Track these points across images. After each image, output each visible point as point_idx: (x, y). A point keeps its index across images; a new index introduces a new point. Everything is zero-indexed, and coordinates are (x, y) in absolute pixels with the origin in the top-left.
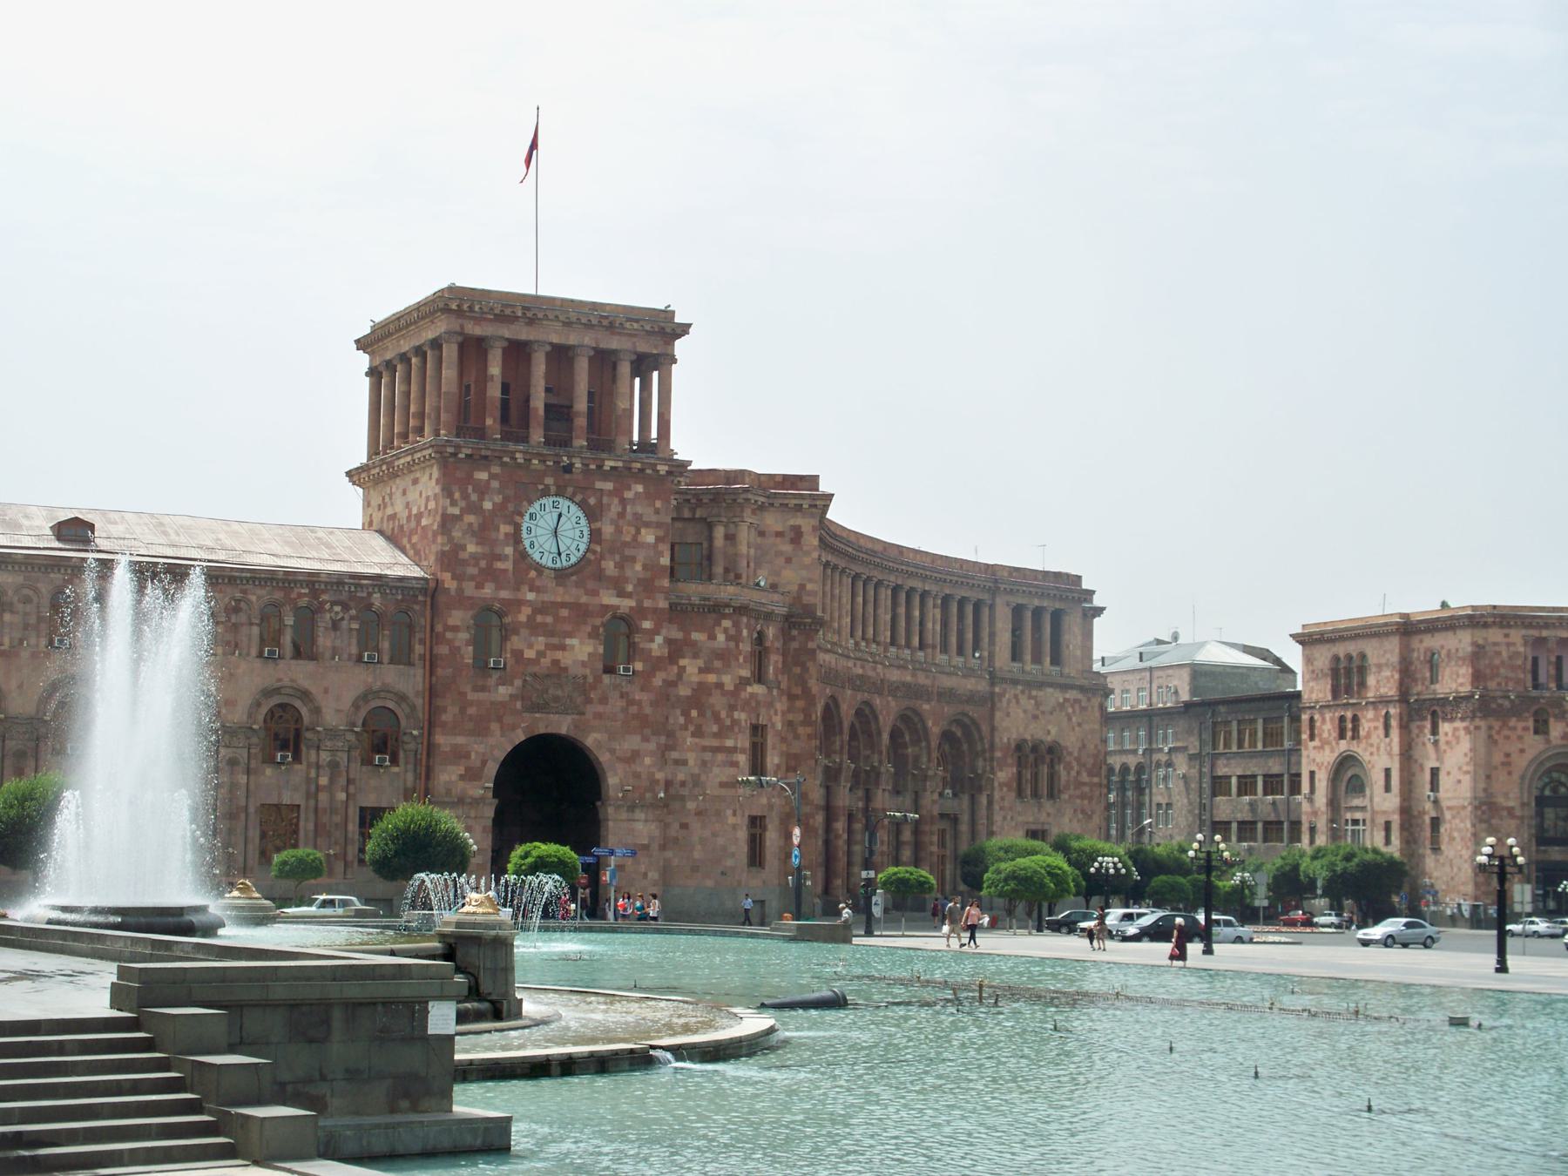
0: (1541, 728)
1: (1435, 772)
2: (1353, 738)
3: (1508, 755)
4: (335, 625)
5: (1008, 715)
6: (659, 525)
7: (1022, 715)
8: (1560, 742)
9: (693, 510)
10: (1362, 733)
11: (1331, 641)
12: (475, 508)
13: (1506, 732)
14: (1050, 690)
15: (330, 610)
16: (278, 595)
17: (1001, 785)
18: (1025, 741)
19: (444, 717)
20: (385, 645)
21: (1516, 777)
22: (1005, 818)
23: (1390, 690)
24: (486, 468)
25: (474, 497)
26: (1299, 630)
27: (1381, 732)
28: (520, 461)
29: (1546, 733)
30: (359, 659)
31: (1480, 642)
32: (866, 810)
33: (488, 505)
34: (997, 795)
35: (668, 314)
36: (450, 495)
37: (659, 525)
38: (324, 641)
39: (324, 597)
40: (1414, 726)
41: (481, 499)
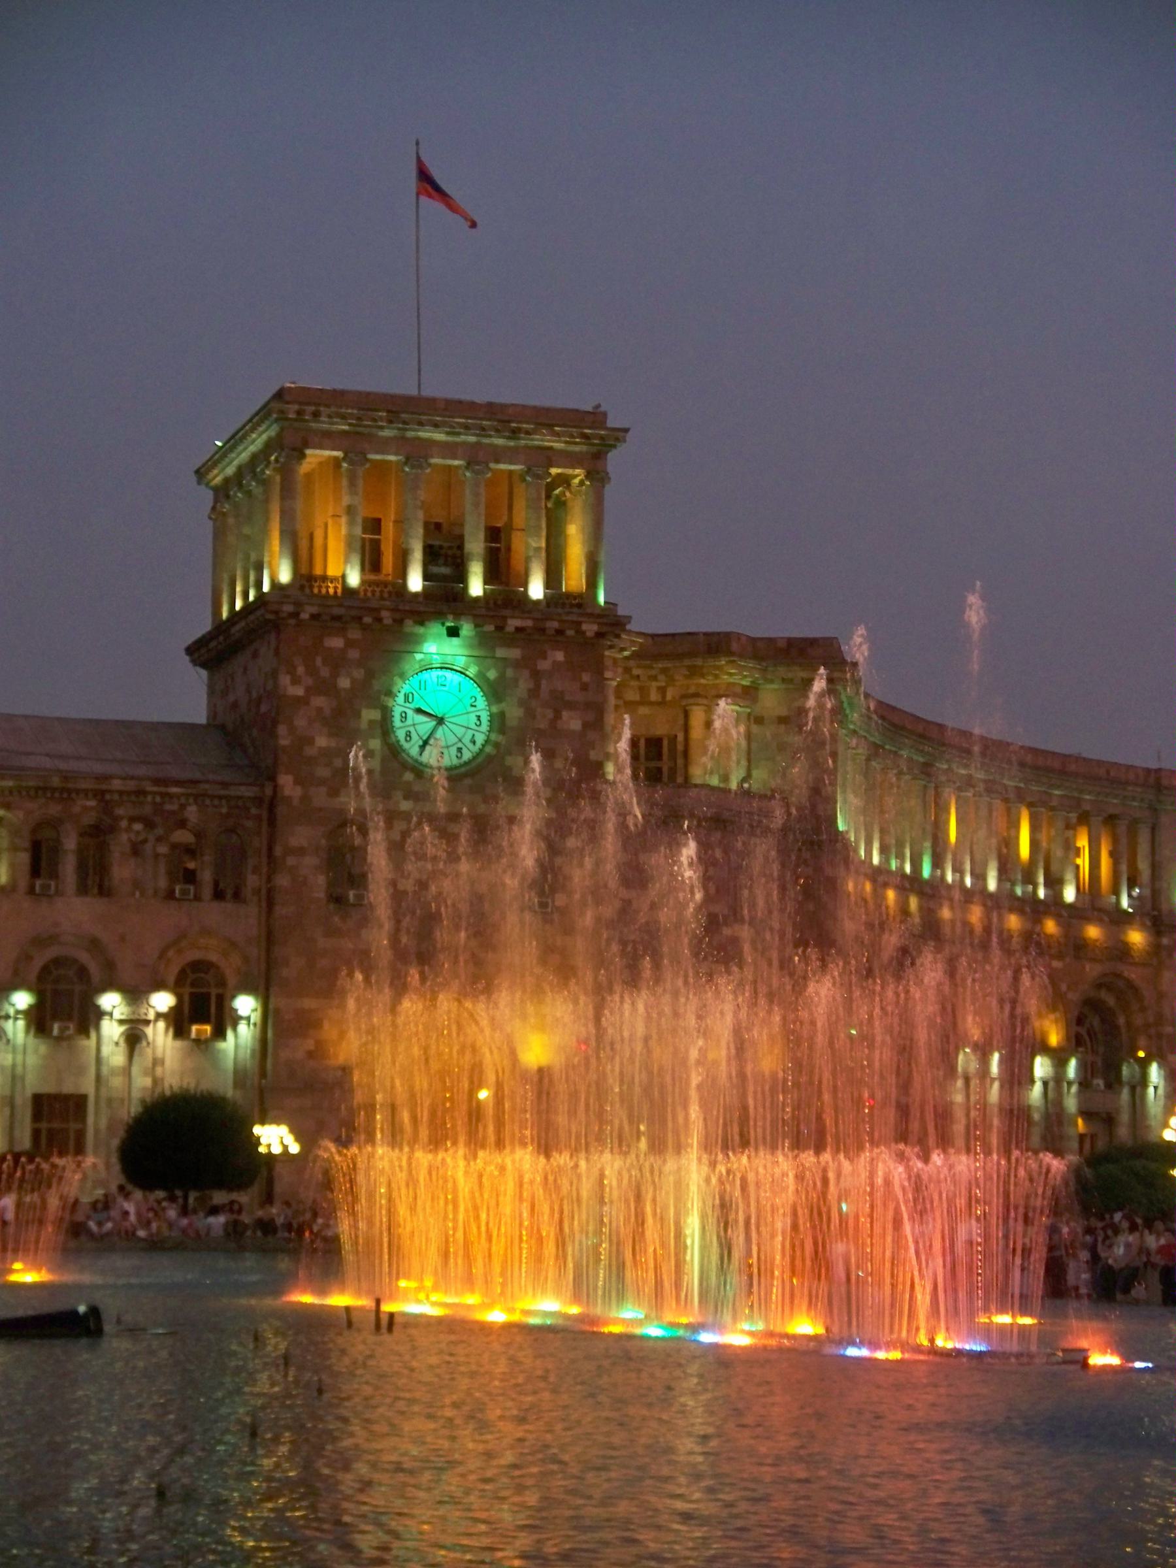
4: (136, 850)
6: (588, 706)
9: (662, 691)
12: (326, 687)
15: (129, 829)
16: (54, 810)
19: (285, 972)
20: (206, 876)
24: (342, 631)
25: (325, 672)
28: (388, 621)
30: (170, 895)
33: (344, 683)
35: (597, 417)
36: (292, 671)
37: (588, 706)
38: (122, 871)
39: (120, 811)
41: (335, 675)
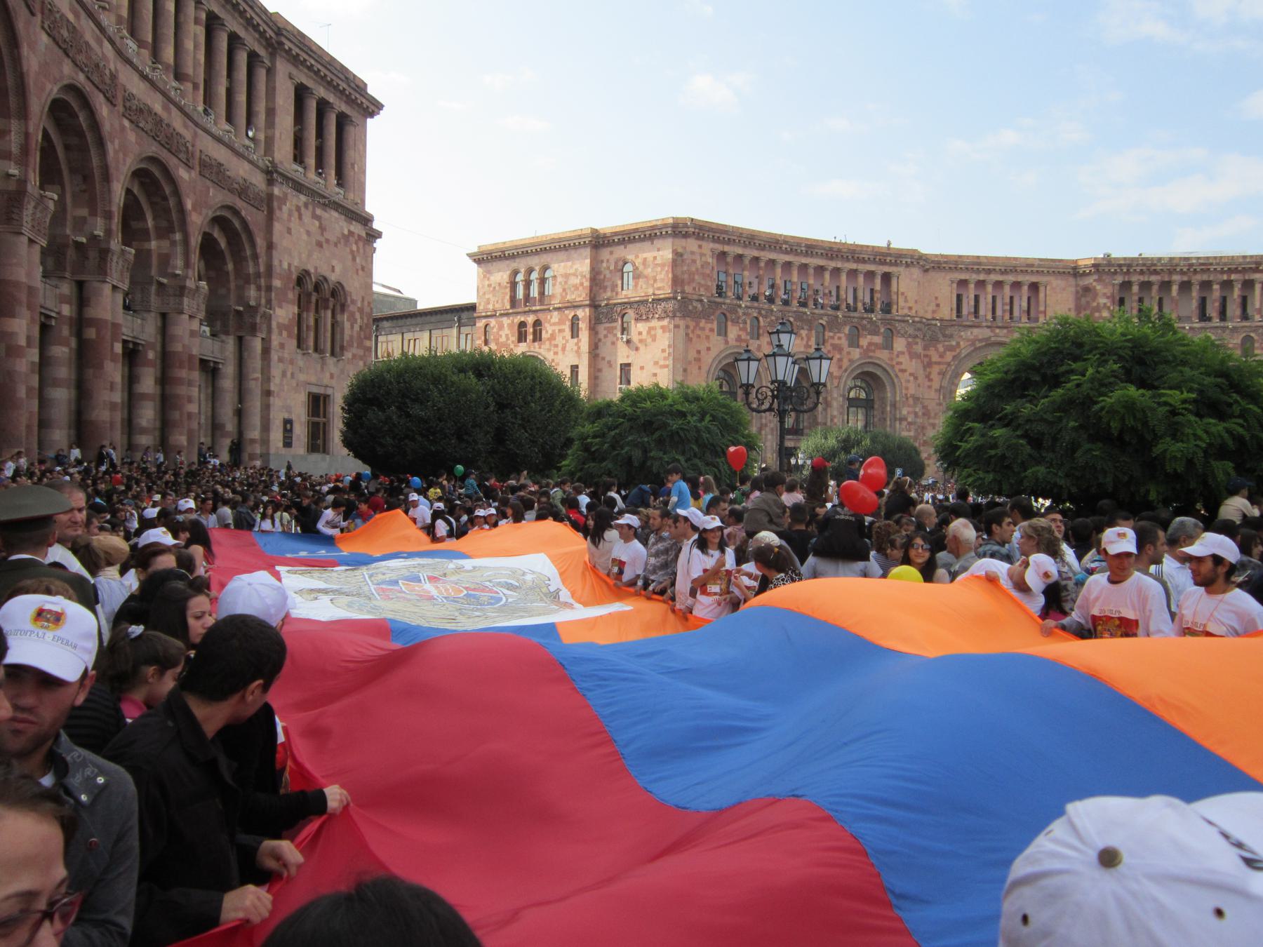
0: (723, 332)
1: (626, 368)
2: (534, 340)
3: (699, 352)
5: (289, 231)
7: (305, 237)
8: (734, 343)
10: (544, 335)
11: (513, 257)
13: (699, 332)
14: (335, 214)
17: (280, 327)
18: (307, 272)
21: (705, 368)
22: (284, 374)
23: (581, 296)
26: (475, 250)
27: (568, 333)
29: (726, 335)
31: (680, 250)
32: (80, 323)
34: (275, 341)
40: (602, 329)
